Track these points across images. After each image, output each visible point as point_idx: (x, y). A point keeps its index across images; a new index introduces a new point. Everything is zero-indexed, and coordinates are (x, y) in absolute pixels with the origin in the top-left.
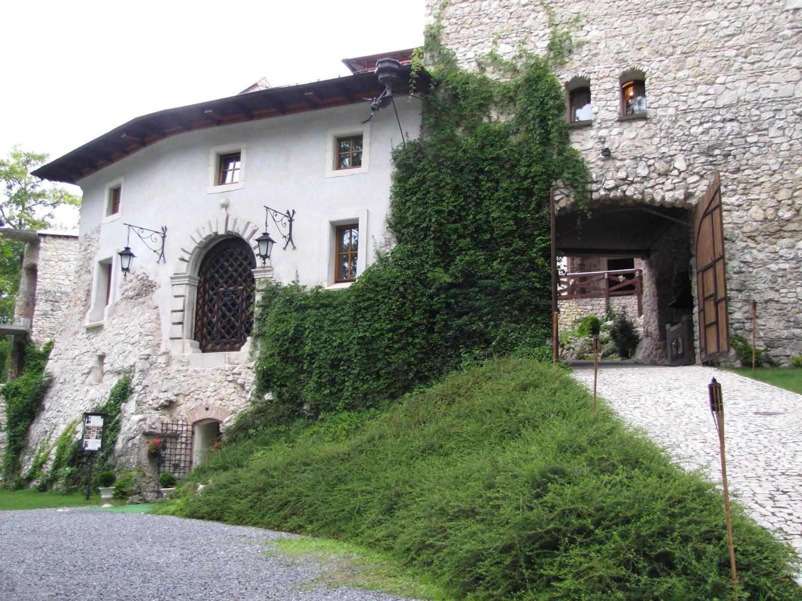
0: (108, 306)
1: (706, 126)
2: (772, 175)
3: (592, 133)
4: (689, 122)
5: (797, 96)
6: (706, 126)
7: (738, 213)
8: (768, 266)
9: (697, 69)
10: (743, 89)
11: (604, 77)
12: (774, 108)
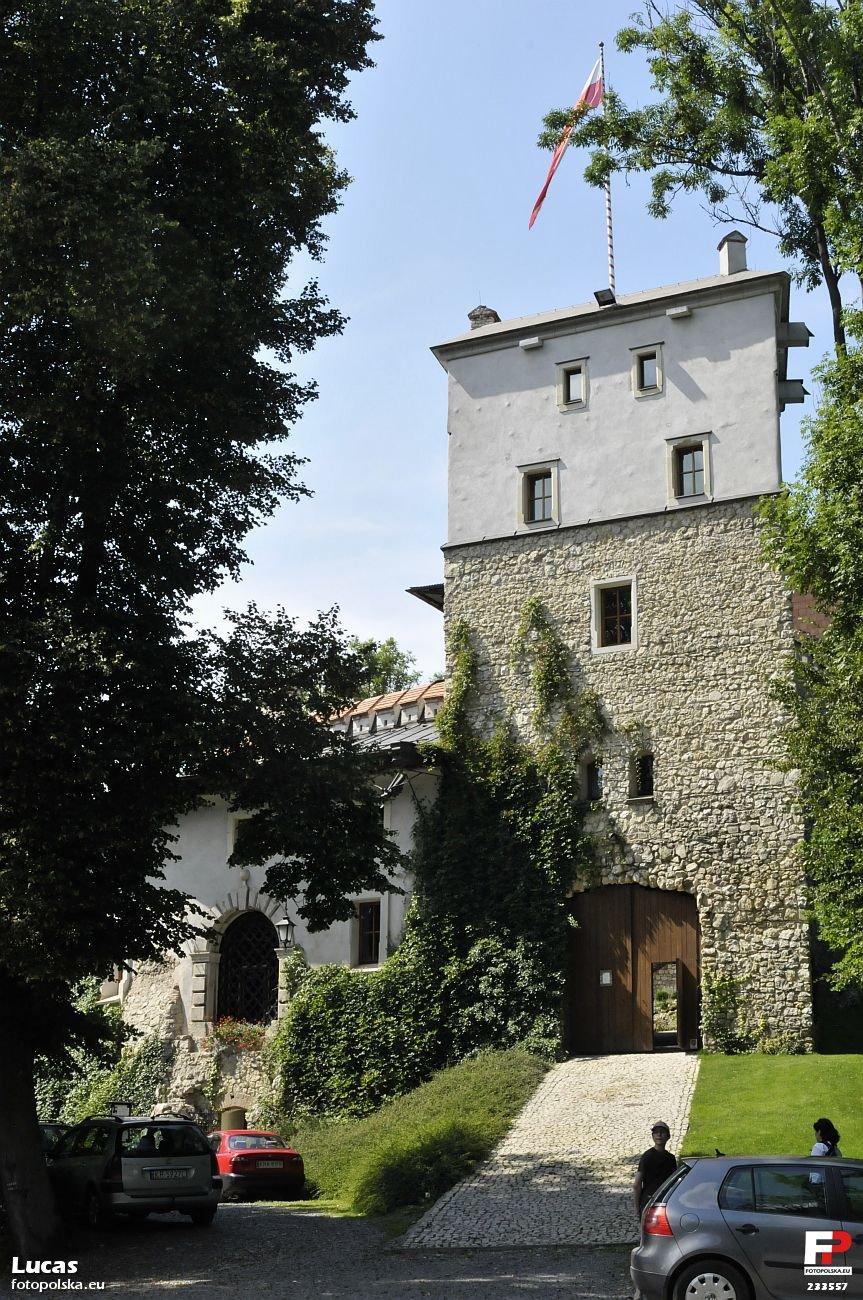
0: (123, 982)
1: (706, 812)
2: (760, 865)
4: (691, 807)
6: (706, 812)
10: (740, 777)
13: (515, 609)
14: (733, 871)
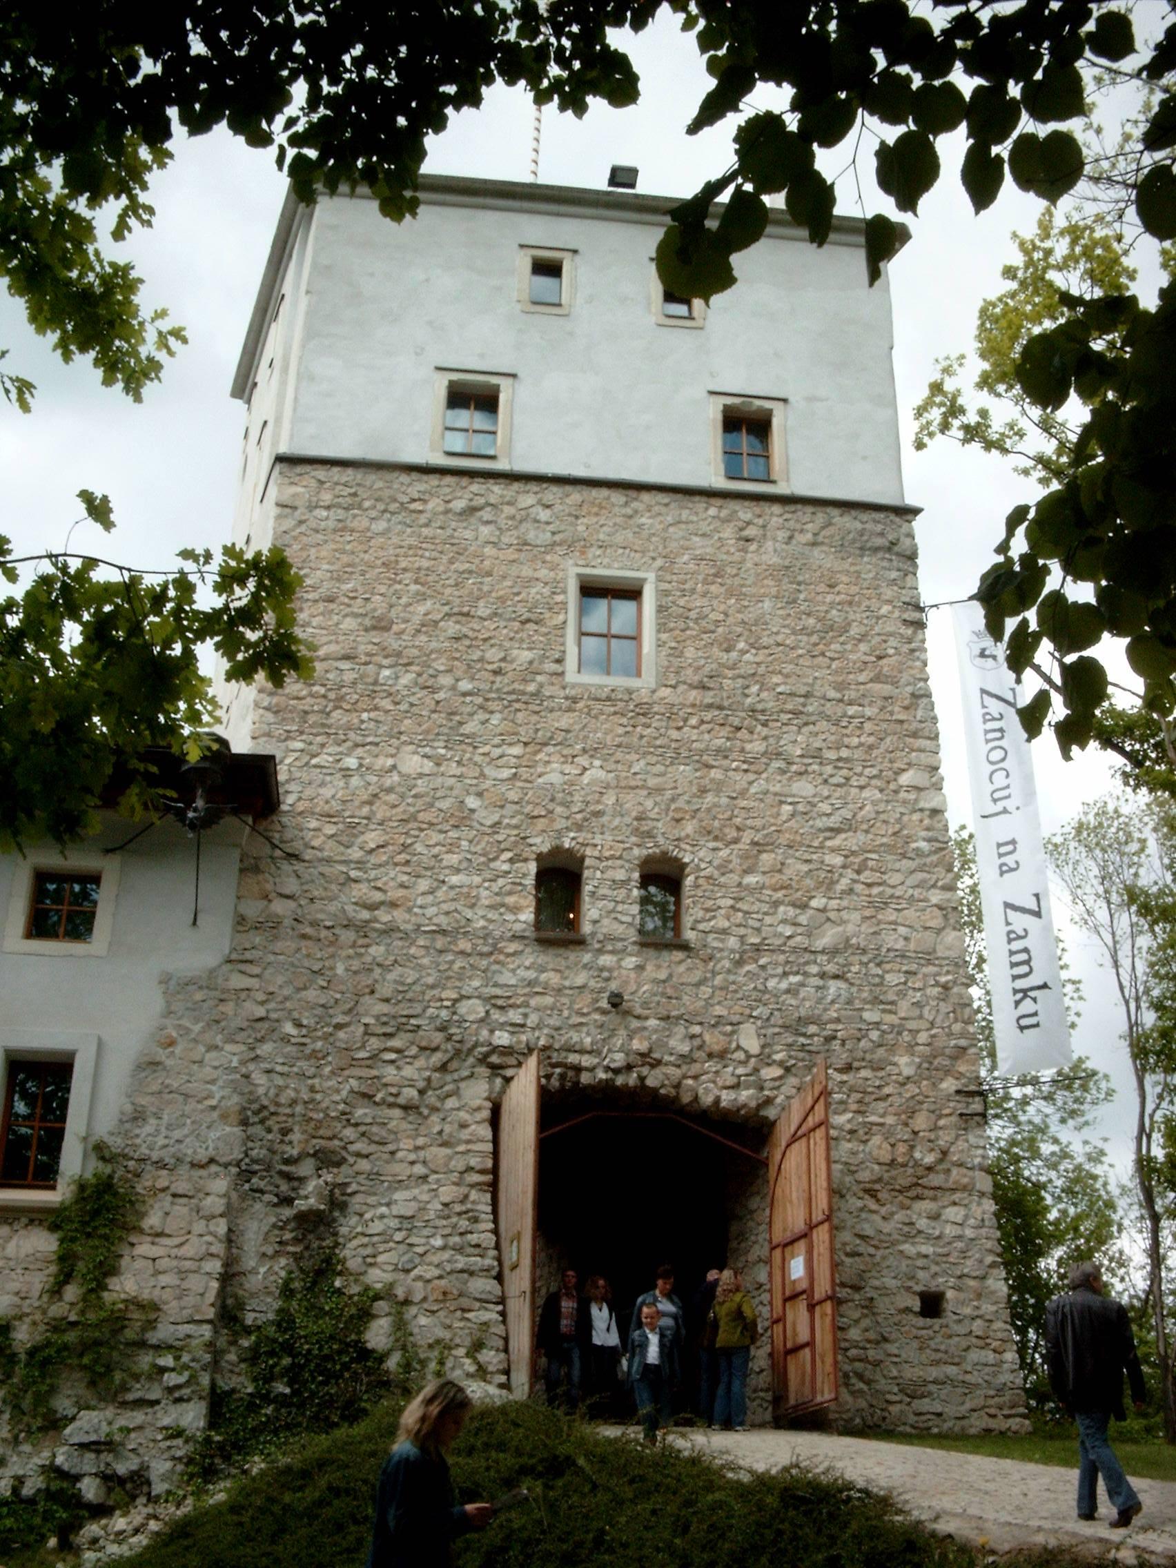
1: (794, 979)
2: (903, 1084)
3: (587, 958)
4: (763, 967)
5: (939, 954)
6: (794, 979)
7: (849, 1145)
8: (901, 1248)
9: (778, 876)
10: (853, 925)
11: (612, 857)
12: (904, 968)
13: (416, 582)
14: (852, 1090)
